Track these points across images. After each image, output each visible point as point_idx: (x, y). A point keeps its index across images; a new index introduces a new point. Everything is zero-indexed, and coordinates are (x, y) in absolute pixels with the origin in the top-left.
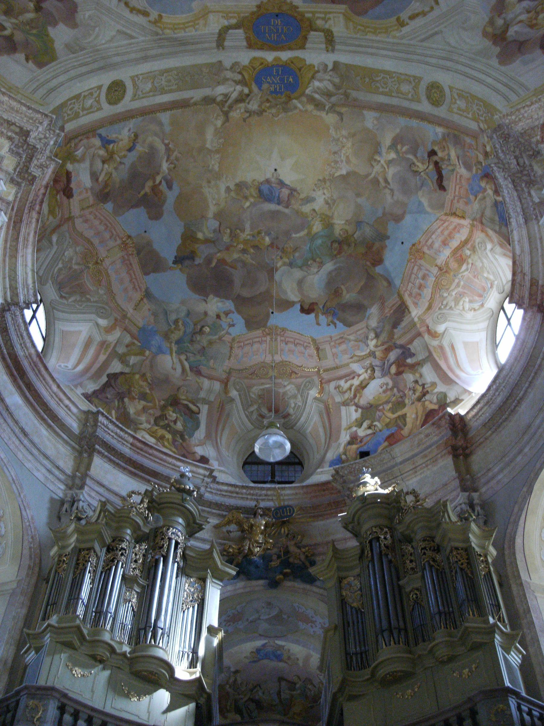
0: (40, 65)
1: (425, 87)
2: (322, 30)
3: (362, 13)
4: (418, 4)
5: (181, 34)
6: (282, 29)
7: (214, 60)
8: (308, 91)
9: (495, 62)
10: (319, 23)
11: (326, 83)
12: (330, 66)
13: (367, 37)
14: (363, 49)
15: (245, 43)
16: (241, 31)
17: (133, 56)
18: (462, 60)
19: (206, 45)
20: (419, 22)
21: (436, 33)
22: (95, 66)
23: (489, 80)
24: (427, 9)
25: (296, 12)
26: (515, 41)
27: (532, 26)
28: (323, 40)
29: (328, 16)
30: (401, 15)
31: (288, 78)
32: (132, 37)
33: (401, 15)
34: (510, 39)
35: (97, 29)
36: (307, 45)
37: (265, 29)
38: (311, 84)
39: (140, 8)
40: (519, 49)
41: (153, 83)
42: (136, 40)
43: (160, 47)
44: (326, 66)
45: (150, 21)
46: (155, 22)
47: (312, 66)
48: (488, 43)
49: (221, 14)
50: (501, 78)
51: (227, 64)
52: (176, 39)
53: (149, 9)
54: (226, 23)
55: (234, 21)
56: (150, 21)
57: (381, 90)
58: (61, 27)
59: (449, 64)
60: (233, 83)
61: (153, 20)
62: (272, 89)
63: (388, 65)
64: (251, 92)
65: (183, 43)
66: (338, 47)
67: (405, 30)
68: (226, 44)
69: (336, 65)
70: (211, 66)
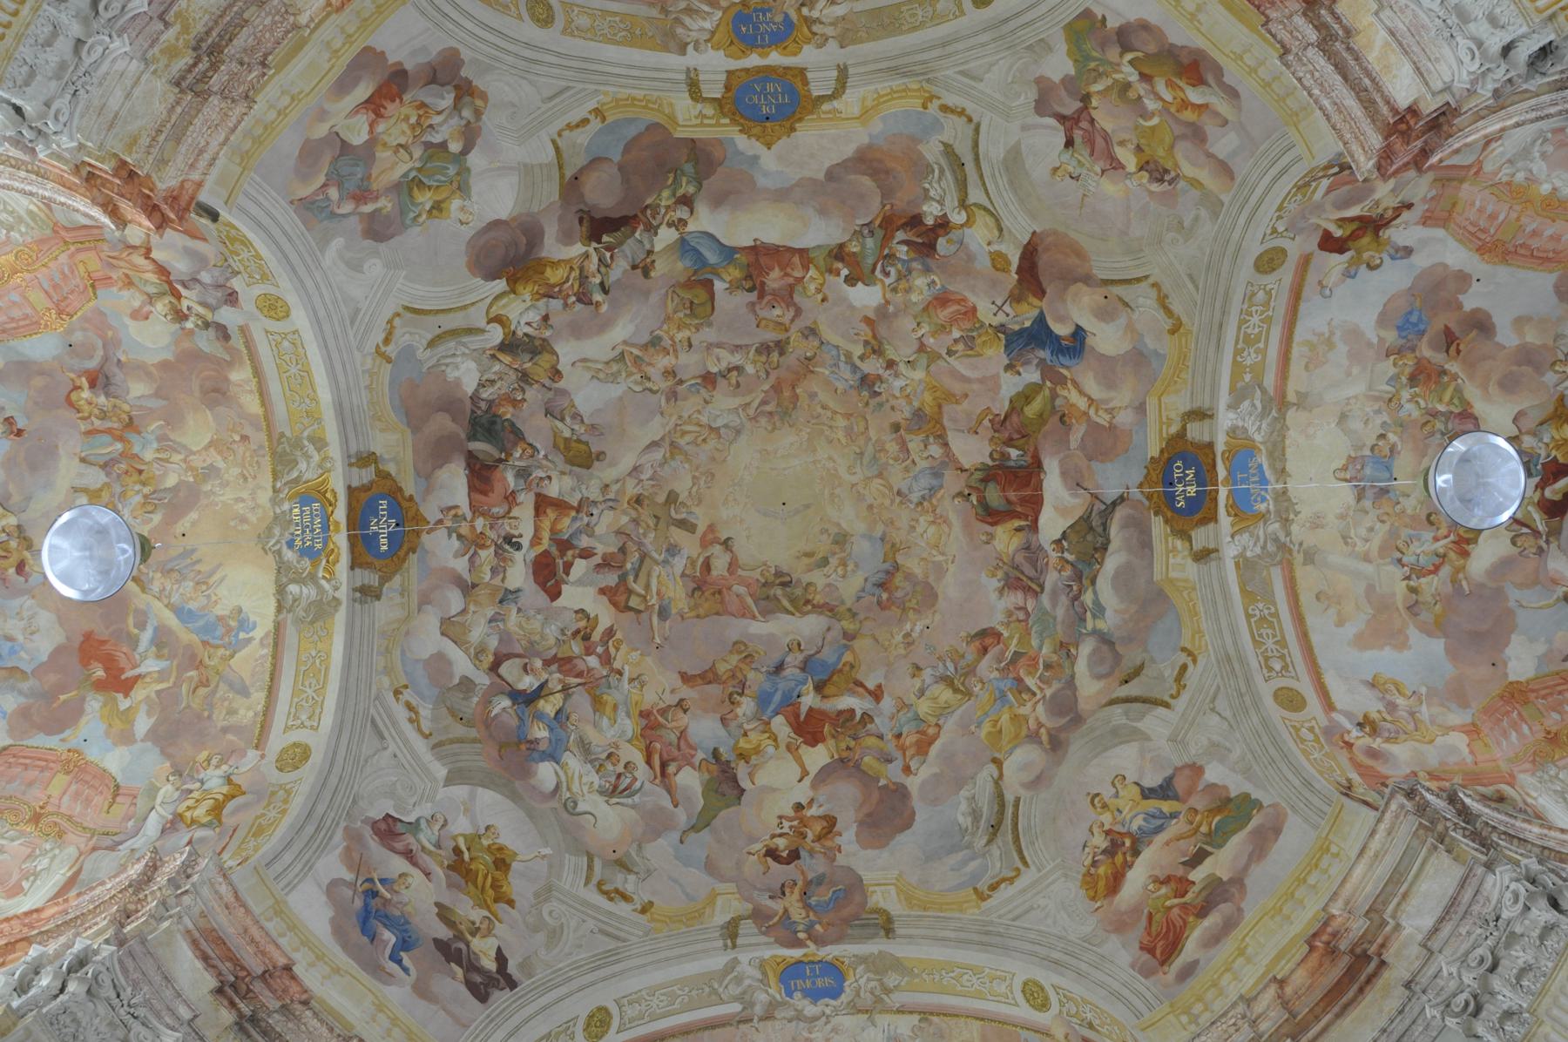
0: (1087, 14)
1: (556, 21)
2: (705, 100)
3: (654, 127)
4: (579, 141)
5: (897, 83)
6: (760, 100)
7: (850, 48)
8: (720, 14)
9: (466, 54)
10: (709, 110)
11: (695, 26)
12: (690, 48)
13: (643, 93)
14: (647, 74)
15: (809, 75)
16: (815, 94)
17: (960, 46)
18: (510, 59)
19: (862, 69)
20: (575, 116)
21: (551, 98)
22: (1012, 24)
23: (469, 25)
24: (566, 133)
25: (742, 125)
26: (442, 85)
27: (423, 105)
28: (702, 87)
29: (698, 121)
30: (600, 125)
31: (748, 30)
32: (962, 73)
33: (600, 125)
34: (449, 88)
35: (1010, 80)
36: (724, 77)
37: (783, 98)
38: (714, 24)
39: (951, 116)
40: (435, 71)
41: (934, 11)
42: (957, 69)
43: (924, 62)
44: (696, 49)
45: (939, 98)
46: (932, 97)
47: (717, 47)
48: (478, 83)
49: (843, 116)
50: (451, 26)
51: (833, 45)
52: (905, 75)
53: (940, 115)
54: (835, 103)
55: (825, 107)
56: (939, 98)
57: (617, 19)
58: (1056, 77)
59: (527, 53)
60: (824, 20)
61: (934, 101)
62: (768, 15)
63: (611, 52)
64: (799, 10)
65: (896, 71)
66: (683, 77)
67: (592, 105)
68: (835, 73)
69: (682, 49)
70: (854, 42)
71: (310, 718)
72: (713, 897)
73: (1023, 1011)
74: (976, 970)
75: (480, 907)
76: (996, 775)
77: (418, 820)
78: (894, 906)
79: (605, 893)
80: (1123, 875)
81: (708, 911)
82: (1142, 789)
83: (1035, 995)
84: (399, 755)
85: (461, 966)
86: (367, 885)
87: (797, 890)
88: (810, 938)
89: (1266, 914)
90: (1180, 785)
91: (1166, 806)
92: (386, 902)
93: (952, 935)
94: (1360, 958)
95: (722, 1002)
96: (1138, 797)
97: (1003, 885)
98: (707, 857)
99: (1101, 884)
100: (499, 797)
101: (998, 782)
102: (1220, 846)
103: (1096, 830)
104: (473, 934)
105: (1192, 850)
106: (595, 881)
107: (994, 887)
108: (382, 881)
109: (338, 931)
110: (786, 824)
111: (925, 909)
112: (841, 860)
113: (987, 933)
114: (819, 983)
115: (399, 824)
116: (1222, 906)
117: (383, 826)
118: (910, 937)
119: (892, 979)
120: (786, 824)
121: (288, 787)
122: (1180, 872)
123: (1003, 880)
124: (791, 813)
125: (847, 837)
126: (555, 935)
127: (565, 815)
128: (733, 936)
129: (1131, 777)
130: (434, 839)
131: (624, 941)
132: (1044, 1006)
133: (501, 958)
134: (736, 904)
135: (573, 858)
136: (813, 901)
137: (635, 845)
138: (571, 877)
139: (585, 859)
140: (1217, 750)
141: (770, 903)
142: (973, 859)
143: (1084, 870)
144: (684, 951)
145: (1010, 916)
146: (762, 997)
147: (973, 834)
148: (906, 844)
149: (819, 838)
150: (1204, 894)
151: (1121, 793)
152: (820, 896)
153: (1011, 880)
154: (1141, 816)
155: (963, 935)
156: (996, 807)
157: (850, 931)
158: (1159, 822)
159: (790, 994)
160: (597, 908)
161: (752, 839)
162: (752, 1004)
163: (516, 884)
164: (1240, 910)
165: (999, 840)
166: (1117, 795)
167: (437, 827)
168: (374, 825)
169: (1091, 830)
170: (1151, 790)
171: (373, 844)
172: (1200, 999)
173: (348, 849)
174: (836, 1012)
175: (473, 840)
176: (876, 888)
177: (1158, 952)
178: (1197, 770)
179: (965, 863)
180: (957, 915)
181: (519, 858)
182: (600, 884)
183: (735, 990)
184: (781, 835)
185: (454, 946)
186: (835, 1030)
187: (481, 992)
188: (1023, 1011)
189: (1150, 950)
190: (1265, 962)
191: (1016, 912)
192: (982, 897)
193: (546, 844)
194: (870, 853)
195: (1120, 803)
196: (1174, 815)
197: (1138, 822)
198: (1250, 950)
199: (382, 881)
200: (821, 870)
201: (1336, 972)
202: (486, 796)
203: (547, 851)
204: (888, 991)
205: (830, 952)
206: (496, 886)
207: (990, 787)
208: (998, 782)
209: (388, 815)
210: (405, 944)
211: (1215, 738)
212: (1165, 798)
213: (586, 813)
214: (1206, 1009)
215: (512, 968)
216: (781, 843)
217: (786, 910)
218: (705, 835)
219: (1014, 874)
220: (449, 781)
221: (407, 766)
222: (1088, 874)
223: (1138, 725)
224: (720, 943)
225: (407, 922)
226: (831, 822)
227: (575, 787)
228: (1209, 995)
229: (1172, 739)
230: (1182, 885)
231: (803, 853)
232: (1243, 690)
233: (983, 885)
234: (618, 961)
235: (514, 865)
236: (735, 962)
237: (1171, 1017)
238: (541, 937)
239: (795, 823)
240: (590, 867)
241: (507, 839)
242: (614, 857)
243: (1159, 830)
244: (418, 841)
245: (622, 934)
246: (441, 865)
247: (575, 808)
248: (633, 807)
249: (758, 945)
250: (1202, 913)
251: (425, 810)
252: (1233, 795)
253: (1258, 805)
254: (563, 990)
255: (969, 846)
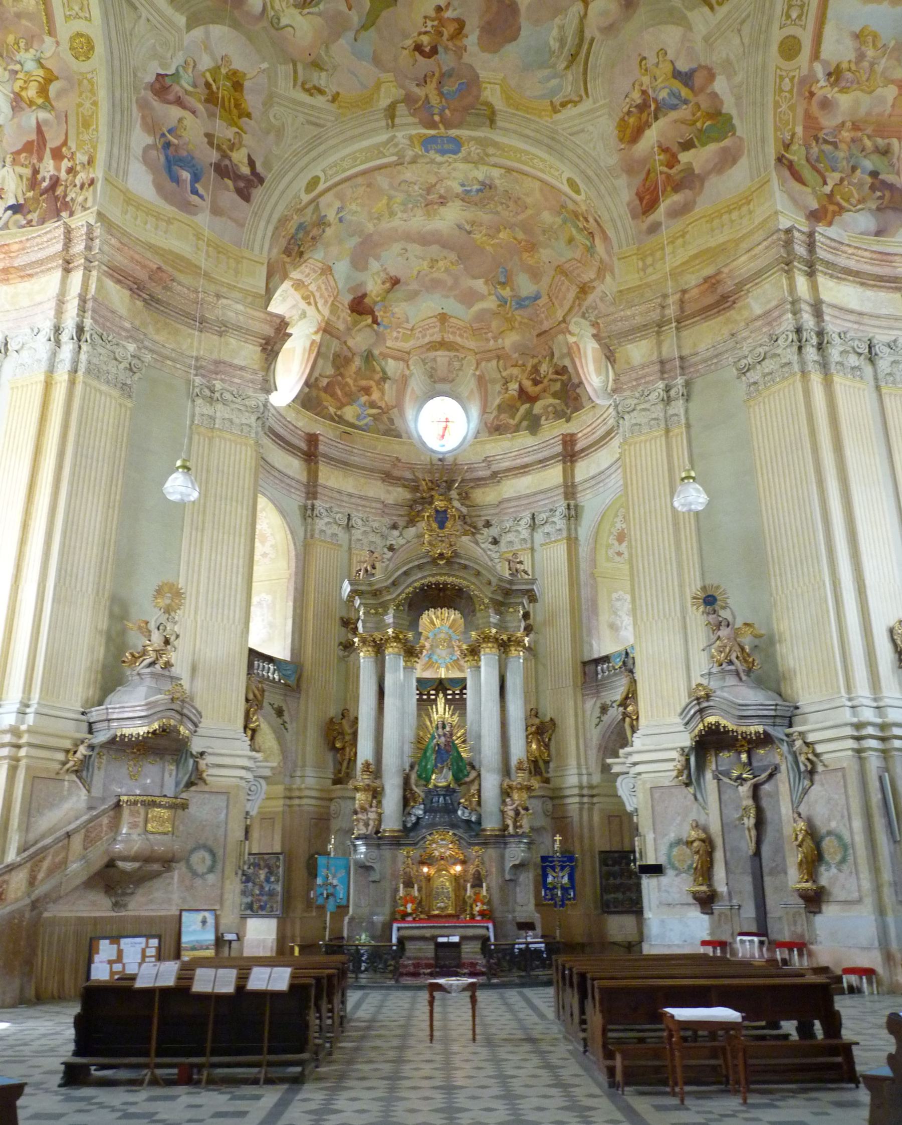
71: (81, 9)
72: (378, 86)
73: (566, 188)
74: (542, 160)
75: (230, 125)
76: (582, 13)
77: (177, 70)
78: (498, 103)
79: (308, 91)
80: (643, 131)
81: (375, 96)
82: (674, 68)
83: (571, 183)
84: (151, 18)
85: (229, 178)
86: (163, 140)
87: (435, 80)
88: (441, 122)
89: (704, 216)
90: (698, 80)
91: (685, 92)
92: (177, 146)
93: (532, 134)
94: (724, 298)
95: (385, 156)
96: (670, 75)
97: (569, 106)
98: (374, 52)
99: (629, 131)
100: (226, 29)
101: (583, 18)
102: (704, 145)
103: (637, 86)
104: (231, 150)
105: (687, 137)
106: (299, 82)
107: (563, 105)
108: (170, 131)
109: (159, 188)
110: (429, 23)
111: (517, 109)
112: (466, 58)
113: (553, 139)
114: (446, 147)
115: (167, 79)
116: (687, 191)
117: (158, 86)
118: (506, 130)
119: (491, 150)
120: (429, 23)
121: (89, 76)
122: (675, 148)
123: (570, 101)
124: (432, 14)
125: (472, 40)
126: (280, 133)
127: (273, 31)
128: (392, 117)
129: (671, 55)
130: (191, 80)
131: (322, 126)
132: (578, 192)
133: (251, 163)
134: (394, 90)
135: (283, 67)
136: (445, 90)
137: (323, 47)
138: (285, 88)
139: (291, 66)
140: (728, 67)
141: (416, 90)
142: (555, 76)
143: (621, 115)
144: (361, 130)
145: (569, 131)
146: (410, 153)
147: (558, 57)
148: (512, 51)
149: (452, 38)
150: (682, 175)
151: (661, 65)
152: (450, 87)
153: (576, 103)
154: (667, 90)
155: (538, 136)
156: (577, 41)
157: (468, 119)
158: (675, 102)
159: (427, 151)
160: (302, 104)
161: (406, 36)
162: (404, 157)
163: (252, 100)
164: (695, 202)
165: (574, 67)
166: (657, 65)
167: (190, 70)
168: (152, 87)
169: (633, 85)
170: (680, 73)
171: (156, 104)
172: (652, 254)
173: (143, 118)
174: (455, 161)
175: (215, 71)
176: (488, 86)
177: (645, 202)
178: (711, 77)
179: (548, 79)
180: (537, 119)
181: (248, 76)
182: (303, 84)
183: (393, 150)
184: (425, 33)
185: (223, 164)
186: (454, 169)
187: (245, 195)
188: (566, 188)
189: (641, 199)
190: (691, 253)
191: (575, 129)
192: (556, 111)
193: (264, 59)
194: (486, 56)
195: (658, 72)
196: (686, 102)
197: (663, 95)
198: (687, 236)
199: (170, 131)
200: (452, 64)
201: (710, 299)
202: (218, 31)
203: (265, 65)
204: (487, 155)
205: (453, 132)
206: (237, 106)
207: (576, 21)
208: (583, 18)
209: (158, 75)
210: (196, 178)
211: (732, 57)
212: (686, 85)
213: (287, 26)
214: (652, 265)
215: (259, 168)
216: (425, 39)
217: (427, 96)
218: (372, 33)
219: (577, 99)
220: (189, 27)
221: (158, 26)
222: (622, 119)
223: (689, 14)
224: (383, 123)
225: (193, 158)
226: (461, 24)
227: (277, 6)
228: (658, 254)
229: (706, 39)
230: (672, 162)
231: (440, 49)
232: (763, 28)
233: (557, 100)
234: (321, 144)
235: (247, 84)
236: (394, 137)
237: (634, 257)
238: (272, 137)
239: (436, 23)
240: (295, 72)
241: (238, 64)
242: (310, 59)
243: (674, 107)
244: (182, 87)
245: (322, 122)
246: (200, 101)
247: (278, 23)
248: (319, 14)
249: (408, 124)
250: (677, 188)
251: (179, 60)
252: (724, 111)
253: (733, 128)
254: (291, 175)
255: (553, 66)
